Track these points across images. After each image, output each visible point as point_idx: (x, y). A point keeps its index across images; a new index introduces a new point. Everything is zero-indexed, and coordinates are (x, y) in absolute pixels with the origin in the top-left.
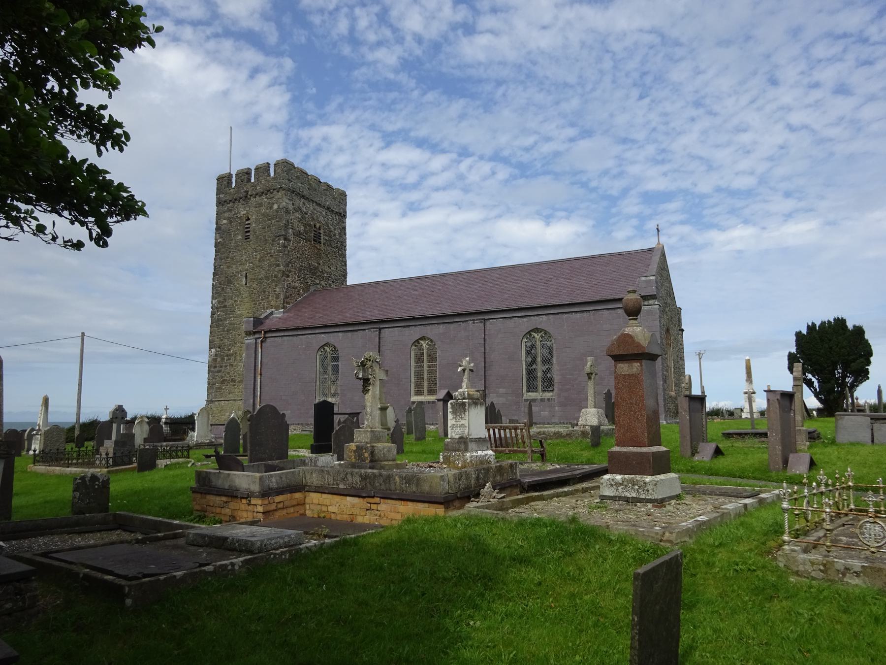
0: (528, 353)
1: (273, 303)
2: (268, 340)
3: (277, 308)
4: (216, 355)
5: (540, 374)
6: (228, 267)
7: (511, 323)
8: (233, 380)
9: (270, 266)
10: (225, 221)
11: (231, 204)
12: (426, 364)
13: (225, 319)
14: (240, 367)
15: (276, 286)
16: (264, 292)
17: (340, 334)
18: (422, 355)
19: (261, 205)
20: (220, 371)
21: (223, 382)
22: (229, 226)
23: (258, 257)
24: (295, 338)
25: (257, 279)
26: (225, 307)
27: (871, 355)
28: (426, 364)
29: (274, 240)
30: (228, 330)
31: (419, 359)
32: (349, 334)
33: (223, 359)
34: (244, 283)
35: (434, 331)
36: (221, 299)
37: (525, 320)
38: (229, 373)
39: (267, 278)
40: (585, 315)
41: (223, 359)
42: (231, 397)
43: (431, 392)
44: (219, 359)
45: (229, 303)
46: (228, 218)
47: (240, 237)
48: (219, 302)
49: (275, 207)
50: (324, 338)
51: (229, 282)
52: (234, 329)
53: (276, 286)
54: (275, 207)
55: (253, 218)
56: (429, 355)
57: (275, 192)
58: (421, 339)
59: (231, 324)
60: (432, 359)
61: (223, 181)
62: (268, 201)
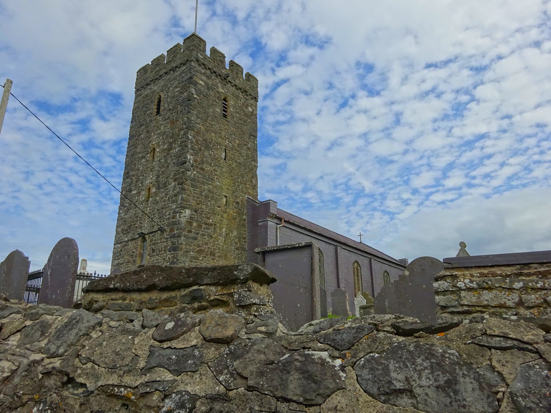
4: (191, 218)
10: (201, 82)
11: (209, 72)
13: (203, 183)
16: (243, 177)
20: (195, 239)
21: (200, 252)
22: (206, 91)
25: (236, 162)
26: (202, 169)
30: (207, 197)
34: (224, 157)
38: (207, 244)
41: (200, 226)
44: (195, 224)
48: (195, 161)
51: (207, 148)
54: (250, 109)
55: (231, 102)
59: (209, 191)
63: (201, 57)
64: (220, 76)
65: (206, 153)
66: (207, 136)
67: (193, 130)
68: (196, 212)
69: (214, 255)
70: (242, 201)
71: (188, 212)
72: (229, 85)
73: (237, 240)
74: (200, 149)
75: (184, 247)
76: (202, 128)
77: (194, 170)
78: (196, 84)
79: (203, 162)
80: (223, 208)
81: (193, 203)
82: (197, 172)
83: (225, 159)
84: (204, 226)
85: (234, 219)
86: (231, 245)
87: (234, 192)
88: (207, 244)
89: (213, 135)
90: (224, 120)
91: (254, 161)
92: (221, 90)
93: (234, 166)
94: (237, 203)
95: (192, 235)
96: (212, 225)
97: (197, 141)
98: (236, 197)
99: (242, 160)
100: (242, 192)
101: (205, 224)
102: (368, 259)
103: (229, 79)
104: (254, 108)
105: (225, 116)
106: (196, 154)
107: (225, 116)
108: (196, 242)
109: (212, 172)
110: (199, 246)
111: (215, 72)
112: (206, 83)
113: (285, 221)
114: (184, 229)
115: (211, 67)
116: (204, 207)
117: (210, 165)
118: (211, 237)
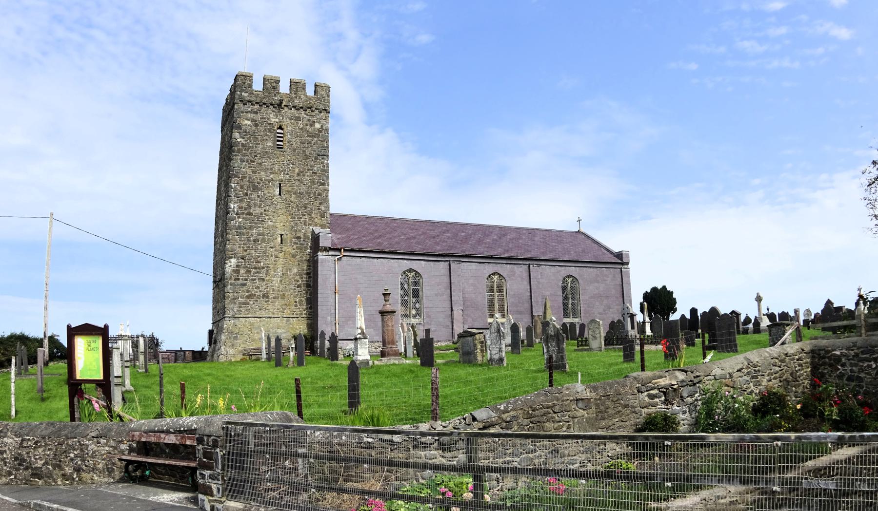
0: (563, 292)
1: (316, 220)
2: (343, 259)
3: (323, 226)
4: (237, 266)
5: (570, 306)
6: (254, 172)
7: (553, 269)
8: (266, 296)
11: (257, 106)
12: (496, 294)
13: (251, 228)
14: (276, 281)
15: (320, 204)
16: (306, 207)
17: (423, 262)
18: (492, 287)
19: (298, 119)
20: (245, 285)
21: (250, 296)
22: (254, 128)
23: (297, 170)
24: (375, 260)
25: (295, 193)
26: (250, 214)
27: (675, 303)
28: (496, 294)
30: (256, 241)
31: (491, 290)
32: (432, 263)
33: (249, 272)
35: (505, 269)
36: (244, 205)
37: (563, 268)
38: (258, 288)
39: (308, 193)
40: (595, 270)
42: (263, 313)
44: (242, 271)
45: (256, 211)
46: (253, 120)
47: (270, 144)
48: (241, 208)
49: (317, 126)
50: (406, 265)
51: (255, 188)
52: (263, 240)
53: (320, 204)
54: (317, 126)
56: (498, 287)
57: (317, 112)
58: (494, 274)
59: (259, 234)
60: (500, 290)
61: (241, 82)
62: (308, 117)
63: (246, 95)
64: (272, 104)
65: (254, 196)
66: (256, 177)
67: (236, 177)
68: (243, 259)
69: (268, 297)
70: (304, 235)
71: (233, 262)
72: (286, 109)
73: (298, 278)
74: (246, 194)
75: (231, 294)
76: (249, 171)
77: (239, 217)
78: (239, 127)
79: (250, 207)
80: (278, 248)
81: (240, 251)
82: (243, 218)
83: (280, 194)
84: (253, 271)
85: (294, 256)
86: (290, 284)
87: (292, 227)
88: (258, 288)
89: (262, 173)
90: (278, 152)
91: (323, 184)
92: (273, 120)
93: (292, 198)
94: (299, 238)
95: (241, 281)
96: (263, 268)
97: (242, 187)
98: (296, 231)
99: (304, 189)
100: (305, 224)
101: (255, 268)
102: (526, 267)
103: (284, 103)
104: (323, 122)
108: (245, 288)
109: (262, 214)
110: (248, 291)
111: (264, 104)
112: (253, 120)
113: (345, 250)
114: (231, 278)
115: (258, 100)
116: (253, 252)
117: (260, 207)
118: (263, 280)
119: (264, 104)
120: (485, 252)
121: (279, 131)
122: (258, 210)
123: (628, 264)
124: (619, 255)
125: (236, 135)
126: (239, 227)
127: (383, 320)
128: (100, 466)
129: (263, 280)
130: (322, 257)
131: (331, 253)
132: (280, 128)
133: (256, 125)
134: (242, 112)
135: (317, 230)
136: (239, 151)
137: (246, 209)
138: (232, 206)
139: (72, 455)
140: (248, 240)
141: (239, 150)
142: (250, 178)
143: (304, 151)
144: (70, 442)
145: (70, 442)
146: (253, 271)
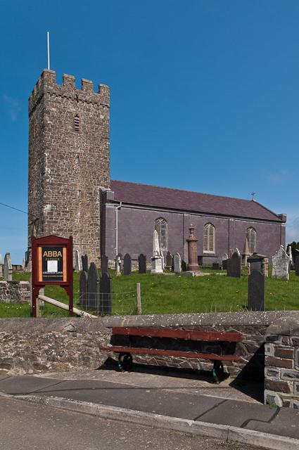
4: (52, 210)
9: (99, 156)
10: (53, 109)
12: (209, 236)
13: (60, 185)
14: (77, 221)
16: (95, 173)
19: (89, 110)
20: (57, 222)
23: (89, 148)
25: (88, 163)
28: (209, 236)
29: (101, 140)
30: (63, 194)
43: (211, 249)
44: (55, 213)
47: (70, 127)
48: (52, 170)
50: (159, 213)
54: (102, 117)
55: (82, 118)
57: (101, 107)
59: (66, 189)
62: (95, 110)
69: (71, 231)
74: (56, 161)
78: (48, 112)
84: (62, 213)
85: (88, 205)
94: (91, 193)
97: (52, 156)
101: (63, 212)
105: (77, 130)
106: (53, 166)
107: (77, 130)
111: (65, 97)
118: (69, 220)
119: (65, 97)
120: (204, 210)
121: (76, 118)
122: (64, 173)
123: (285, 222)
124: (281, 216)
125: (47, 118)
126: (52, 184)
127: (189, 245)
128: (77, 355)
129: (69, 220)
130: (108, 205)
131: (113, 204)
132: (77, 116)
133: (61, 113)
134: (50, 101)
135: (104, 189)
136: (49, 130)
137: (56, 172)
138: (46, 169)
139: (46, 347)
140: (59, 193)
141: (49, 129)
142: (58, 150)
143: (93, 135)
144: (44, 336)
145: (44, 336)
146: (62, 213)
